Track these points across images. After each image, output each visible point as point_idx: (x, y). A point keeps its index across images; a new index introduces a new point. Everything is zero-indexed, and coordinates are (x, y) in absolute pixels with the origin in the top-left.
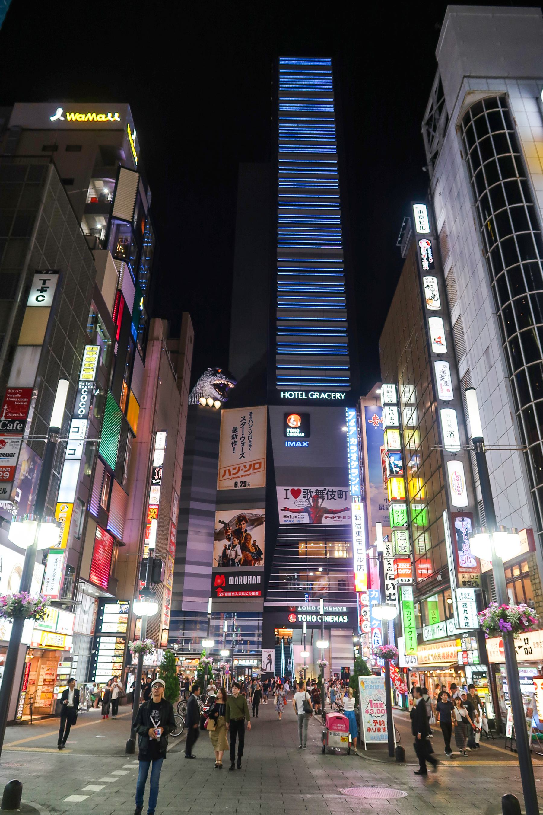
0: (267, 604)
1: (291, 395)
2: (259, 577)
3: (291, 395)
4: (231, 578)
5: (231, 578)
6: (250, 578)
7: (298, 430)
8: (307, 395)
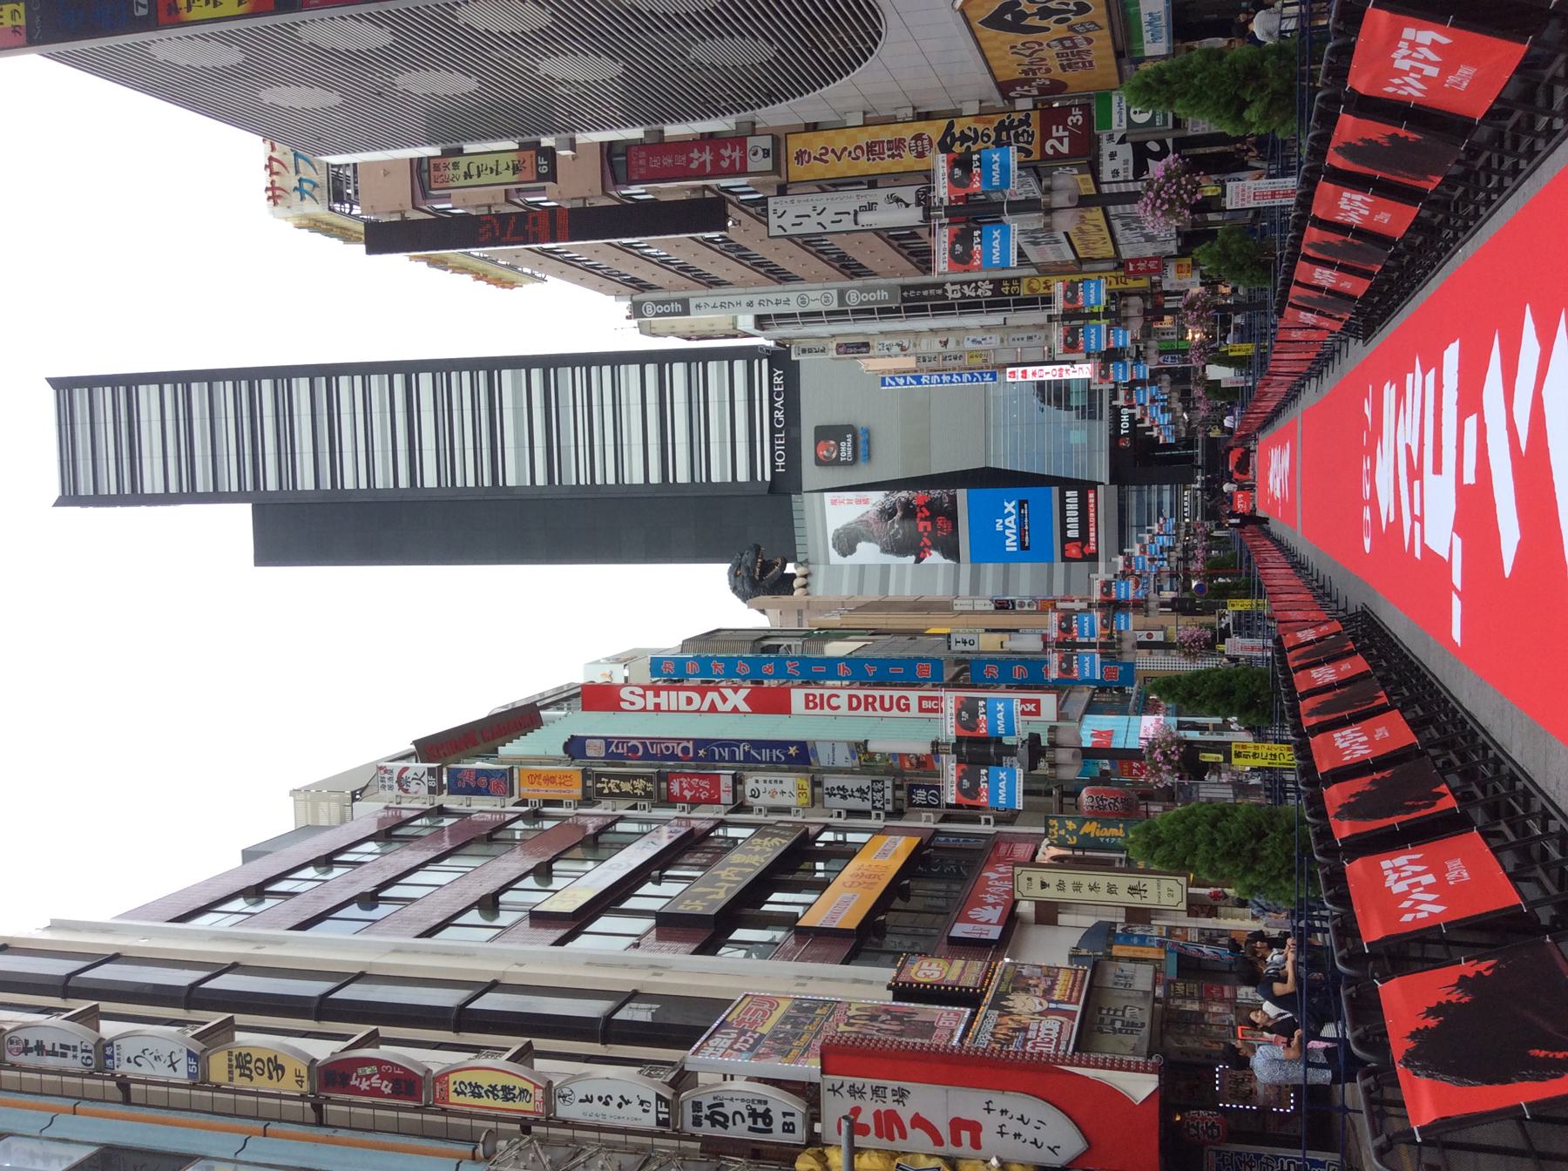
0: (1105, 478)
1: (780, 456)
2: (1068, 494)
3: (780, 456)
4: (1070, 534)
5: (1070, 534)
6: (1069, 507)
7: (843, 444)
8: (780, 431)
